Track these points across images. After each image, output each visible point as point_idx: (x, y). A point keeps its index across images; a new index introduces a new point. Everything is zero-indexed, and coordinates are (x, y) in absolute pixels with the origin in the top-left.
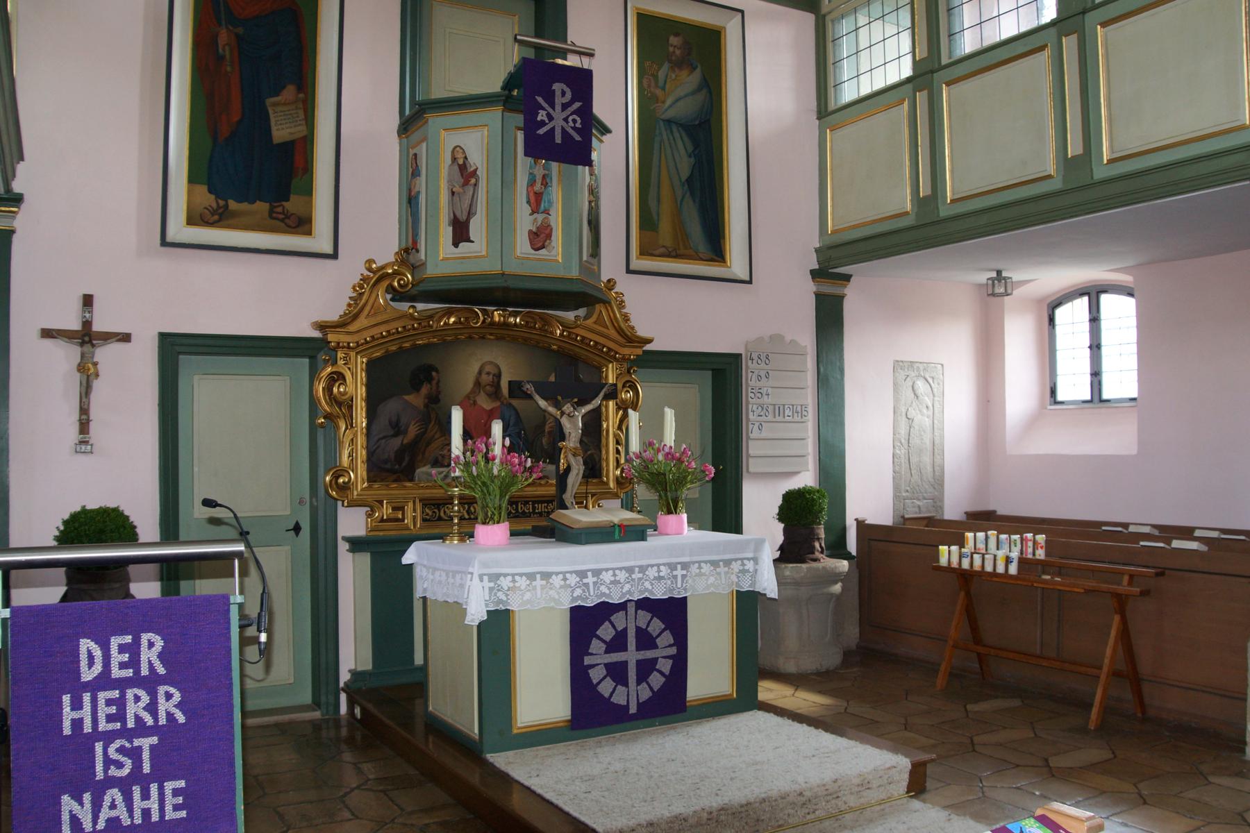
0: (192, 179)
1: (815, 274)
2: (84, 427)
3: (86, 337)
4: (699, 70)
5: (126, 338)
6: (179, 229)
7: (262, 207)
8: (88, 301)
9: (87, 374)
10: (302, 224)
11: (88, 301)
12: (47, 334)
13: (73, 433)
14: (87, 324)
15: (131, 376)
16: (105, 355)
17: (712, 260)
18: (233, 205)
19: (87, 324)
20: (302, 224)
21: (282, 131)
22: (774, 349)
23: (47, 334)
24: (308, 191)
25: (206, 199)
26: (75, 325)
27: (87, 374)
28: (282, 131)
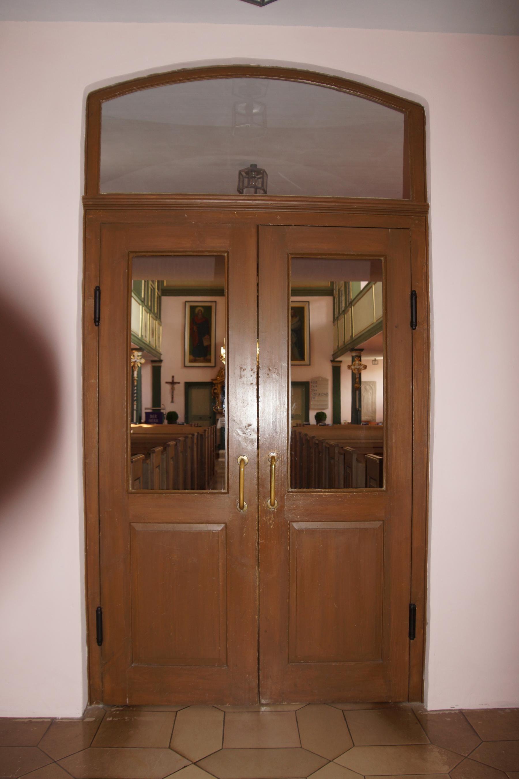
0: (190, 354)
1: (332, 361)
2: (172, 398)
3: (173, 383)
4: (298, 318)
5: (179, 383)
6: (187, 364)
7: (202, 358)
8: (173, 377)
9: (173, 390)
10: (209, 361)
11: (173, 377)
12: (167, 383)
13: (170, 400)
14: (173, 380)
15: (180, 389)
16: (176, 386)
17: (301, 360)
18: (197, 358)
19: (173, 380)
20: (209, 361)
21: (205, 344)
22: (319, 381)
23: (167, 383)
24: (210, 354)
25: (192, 357)
26: (170, 381)
27: (173, 390)
28: (205, 344)
